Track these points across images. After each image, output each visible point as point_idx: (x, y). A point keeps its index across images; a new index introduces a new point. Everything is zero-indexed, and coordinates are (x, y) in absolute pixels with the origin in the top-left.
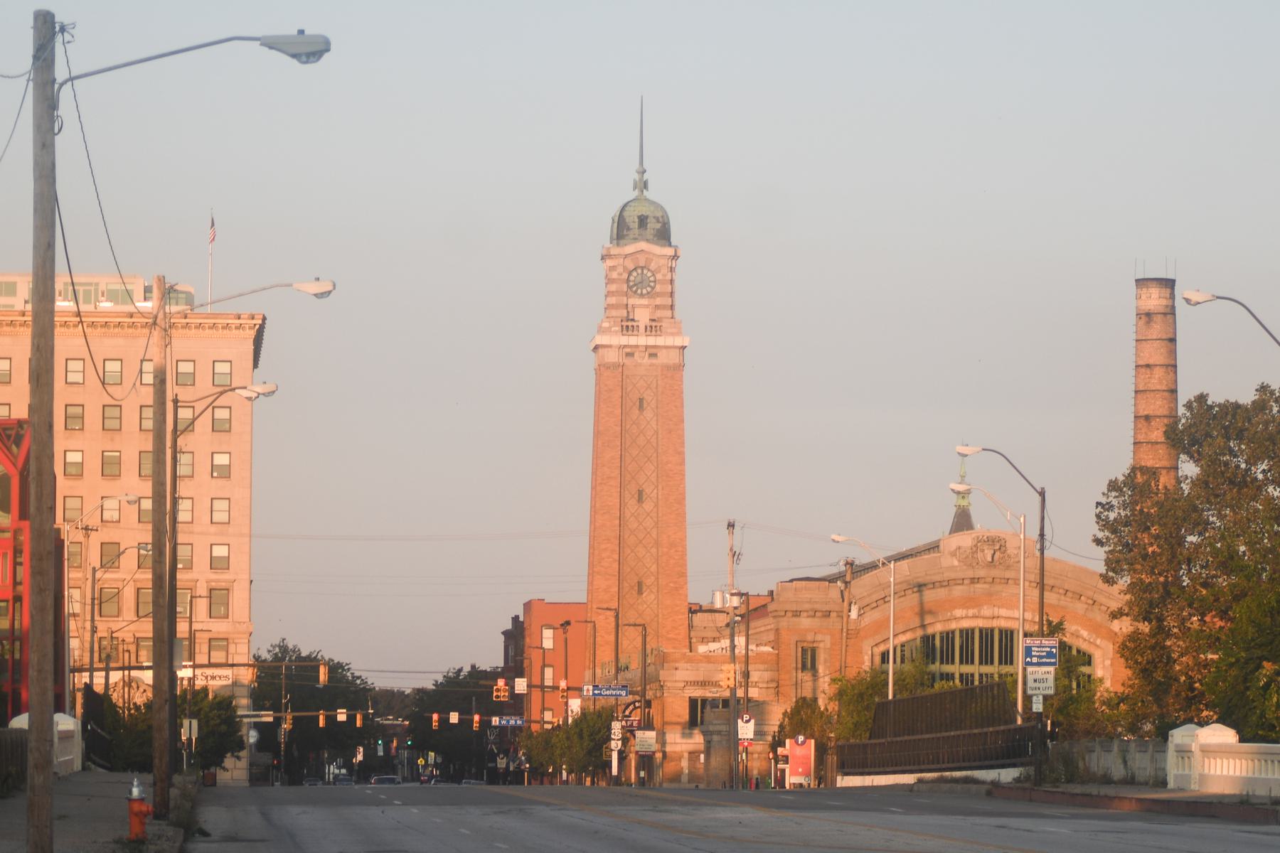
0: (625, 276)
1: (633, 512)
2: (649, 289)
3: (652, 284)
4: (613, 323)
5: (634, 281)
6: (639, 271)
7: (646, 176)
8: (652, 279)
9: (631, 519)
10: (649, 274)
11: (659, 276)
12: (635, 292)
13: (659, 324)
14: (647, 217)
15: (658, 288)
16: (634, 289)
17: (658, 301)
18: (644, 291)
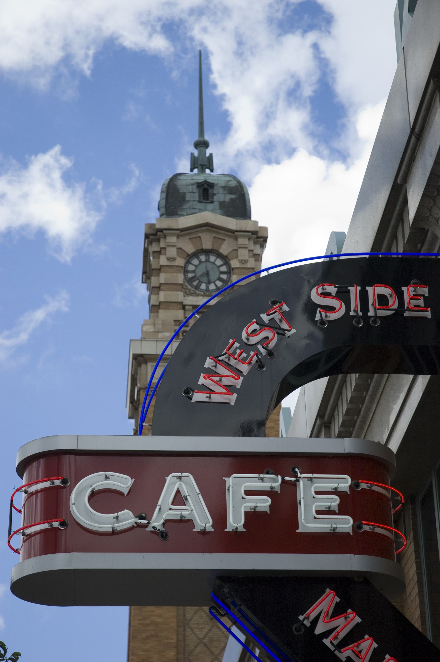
0: (180, 262)
1: (201, 636)
2: (219, 284)
3: (224, 277)
4: (160, 326)
5: (194, 272)
6: (203, 258)
7: (208, 152)
8: (224, 269)
9: (199, 649)
10: (219, 262)
11: (234, 263)
12: (197, 287)
14: (212, 185)
16: (195, 283)
18: (212, 287)
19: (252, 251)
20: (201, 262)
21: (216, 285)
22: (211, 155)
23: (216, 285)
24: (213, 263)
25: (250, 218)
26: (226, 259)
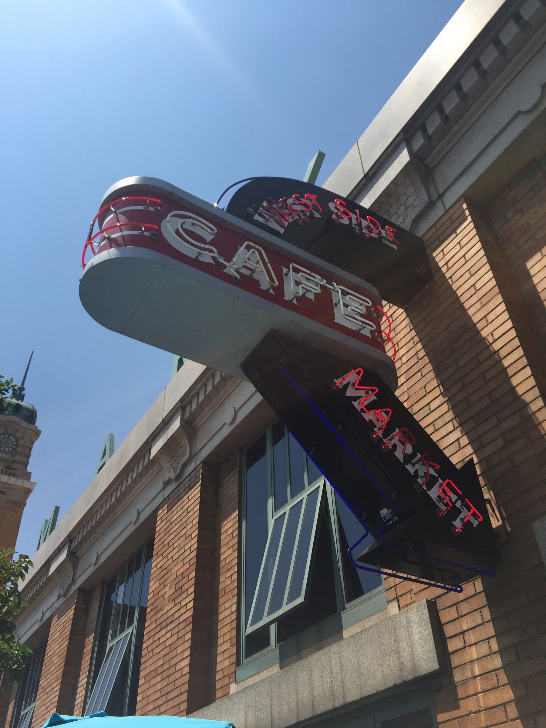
2: (11, 449)
3: (14, 447)
6: (7, 436)
7: (23, 393)
8: (15, 443)
10: (14, 440)
11: (21, 442)
13: (13, 471)
15: (19, 449)
17: (17, 458)
19: (31, 439)
20: (5, 437)
21: (9, 449)
22: (24, 394)
23: (9, 449)
24: (11, 439)
25: (34, 424)
26: (17, 439)
